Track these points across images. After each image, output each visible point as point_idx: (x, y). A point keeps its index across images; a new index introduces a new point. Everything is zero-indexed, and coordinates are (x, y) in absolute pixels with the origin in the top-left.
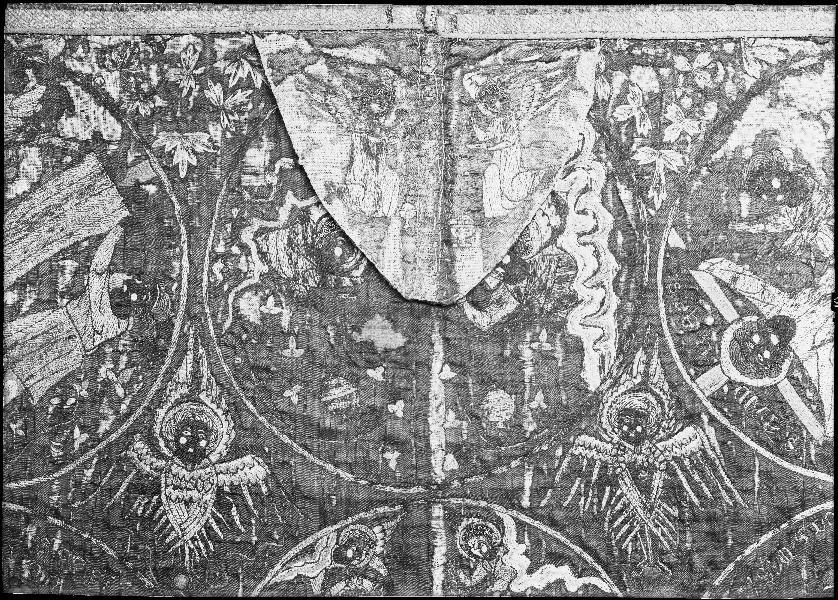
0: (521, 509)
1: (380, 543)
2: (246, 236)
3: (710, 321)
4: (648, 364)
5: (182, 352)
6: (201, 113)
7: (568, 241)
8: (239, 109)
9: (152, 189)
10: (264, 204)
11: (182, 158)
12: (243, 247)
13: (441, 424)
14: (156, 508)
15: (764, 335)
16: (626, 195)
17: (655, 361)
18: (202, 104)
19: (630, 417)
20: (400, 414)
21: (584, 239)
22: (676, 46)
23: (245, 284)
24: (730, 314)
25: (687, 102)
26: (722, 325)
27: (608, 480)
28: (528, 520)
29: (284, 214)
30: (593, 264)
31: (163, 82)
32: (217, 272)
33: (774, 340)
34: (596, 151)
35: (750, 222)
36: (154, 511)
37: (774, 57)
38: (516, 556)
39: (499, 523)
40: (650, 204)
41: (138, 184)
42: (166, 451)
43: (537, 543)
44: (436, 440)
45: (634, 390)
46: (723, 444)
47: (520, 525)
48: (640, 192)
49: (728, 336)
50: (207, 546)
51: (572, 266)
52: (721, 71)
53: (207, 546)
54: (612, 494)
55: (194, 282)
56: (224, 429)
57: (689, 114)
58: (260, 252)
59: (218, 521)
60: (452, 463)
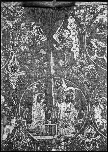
0: (65, 78)
1: (44, 84)
2: (21, 37)
3: (93, 48)
4: (84, 55)
5: (12, 55)
6: (14, 18)
7: (71, 36)
8: (20, 17)
9: (6, 30)
10: (24, 32)
11: (11, 25)
12: (21, 39)
13: (52, 65)
14: (8, 80)
15: (102, 50)
16: (80, 29)
17: (85, 54)
18: (14, 16)
19: (82, 64)
20: (46, 64)
21: (74, 36)
22: (87, 6)
23: (22, 44)
24: (96, 47)
25: (89, 15)
26: (95, 49)
27: (78, 73)
28: (66, 80)
29: (27, 34)
30: (75, 40)
31: (8, 13)
32: (17, 43)
33: (103, 51)
34: (75, 23)
35: (99, 33)
36: (8, 80)
37: (102, 7)
38: (64, 85)
39: (62, 81)
40: (83, 30)
41: (4, 29)
42: (10, 71)
43: (68, 84)
44: (52, 68)
45: (82, 59)
46: (96, 67)
47: (65, 80)
48: (82, 29)
49: (96, 51)
50: (17, 85)
51: (72, 40)
52: (94, 10)
53: (17, 85)
54: (79, 75)
55: (13, 44)
56: (19, 67)
57: (89, 16)
58: (24, 39)
59: (18, 81)
60: (54, 72)
